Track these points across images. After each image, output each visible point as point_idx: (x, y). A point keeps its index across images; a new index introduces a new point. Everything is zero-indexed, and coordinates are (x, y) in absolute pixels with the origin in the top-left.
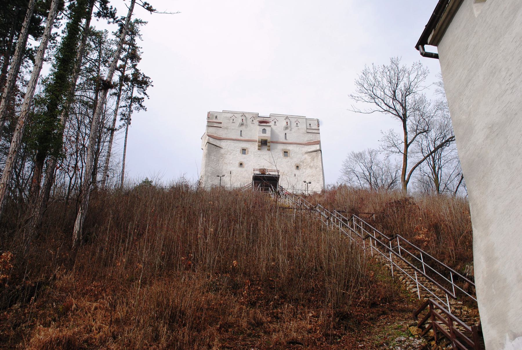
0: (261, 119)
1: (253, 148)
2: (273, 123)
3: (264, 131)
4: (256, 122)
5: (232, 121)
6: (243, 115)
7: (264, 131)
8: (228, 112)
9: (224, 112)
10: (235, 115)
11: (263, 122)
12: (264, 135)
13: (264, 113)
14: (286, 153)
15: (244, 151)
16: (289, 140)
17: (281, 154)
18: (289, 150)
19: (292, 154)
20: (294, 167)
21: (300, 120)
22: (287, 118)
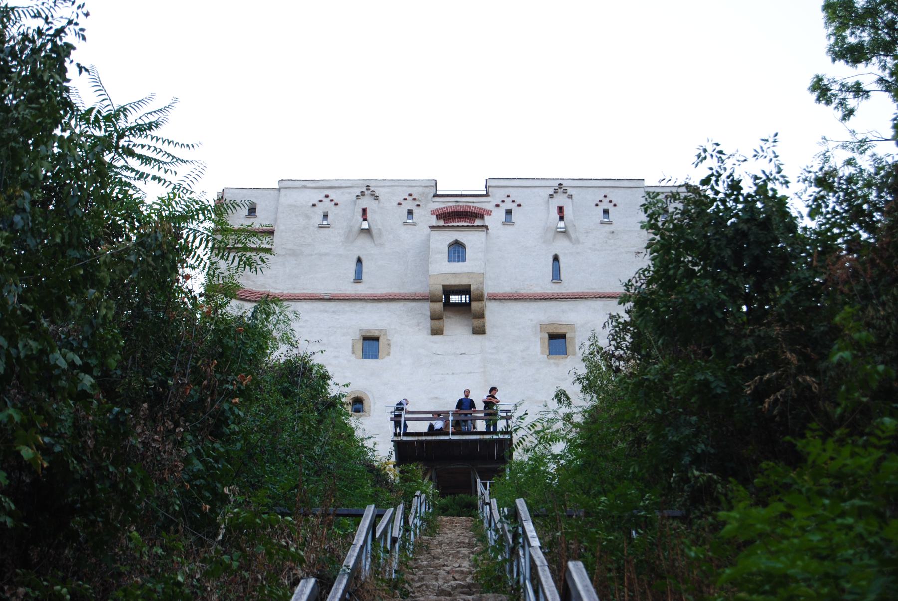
0: (449, 204)
1: (404, 328)
2: (500, 214)
3: (457, 250)
4: (425, 218)
5: (318, 220)
6: (368, 190)
7: (457, 250)
8: (304, 185)
9: (286, 185)
10: (333, 194)
11: (460, 215)
12: (457, 267)
13: (461, 179)
15: (371, 344)
16: (569, 285)
17: (537, 346)
18: (572, 326)
22: (560, 188)
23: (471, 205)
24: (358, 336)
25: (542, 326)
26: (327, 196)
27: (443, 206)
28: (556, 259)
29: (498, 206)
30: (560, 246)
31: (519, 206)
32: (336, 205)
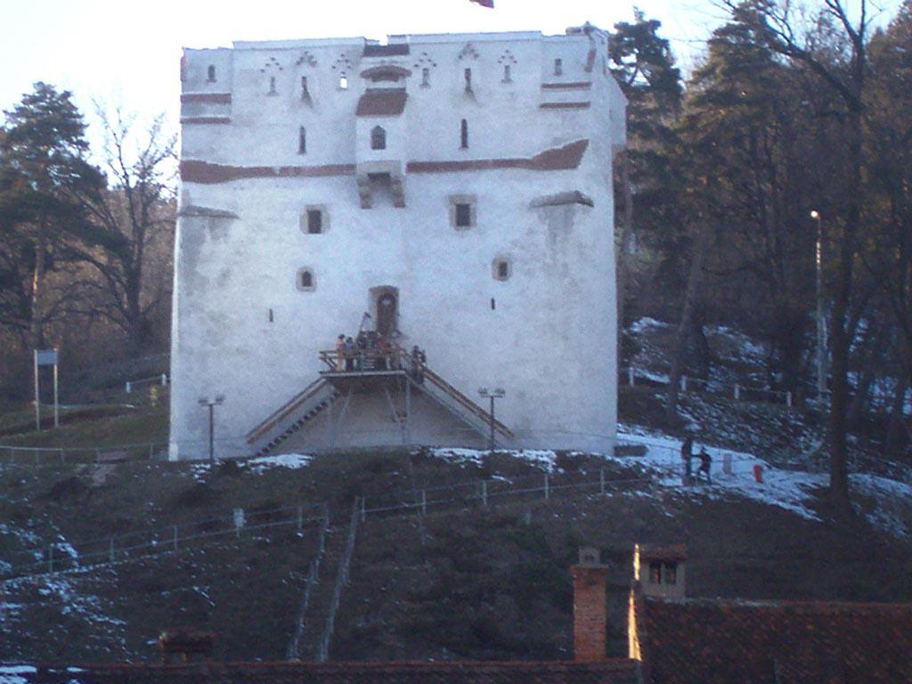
5: (266, 86)
8: (253, 48)
9: (241, 48)
10: (278, 57)
14: (463, 215)
16: (475, 153)
17: (445, 218)
19: (482, 216)
20: (489, 273)
21: (517, 52)
23: (396, 65)
24: (304, 212)
25: (451, 198)
26: (273, 59)
27: (372, 66)
28: (464, 123)
29: (416, 66)
30: (467, 111)
31: (435, 65)
32: (281, 69)
